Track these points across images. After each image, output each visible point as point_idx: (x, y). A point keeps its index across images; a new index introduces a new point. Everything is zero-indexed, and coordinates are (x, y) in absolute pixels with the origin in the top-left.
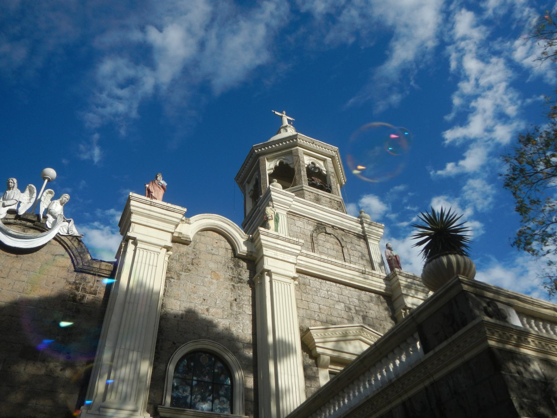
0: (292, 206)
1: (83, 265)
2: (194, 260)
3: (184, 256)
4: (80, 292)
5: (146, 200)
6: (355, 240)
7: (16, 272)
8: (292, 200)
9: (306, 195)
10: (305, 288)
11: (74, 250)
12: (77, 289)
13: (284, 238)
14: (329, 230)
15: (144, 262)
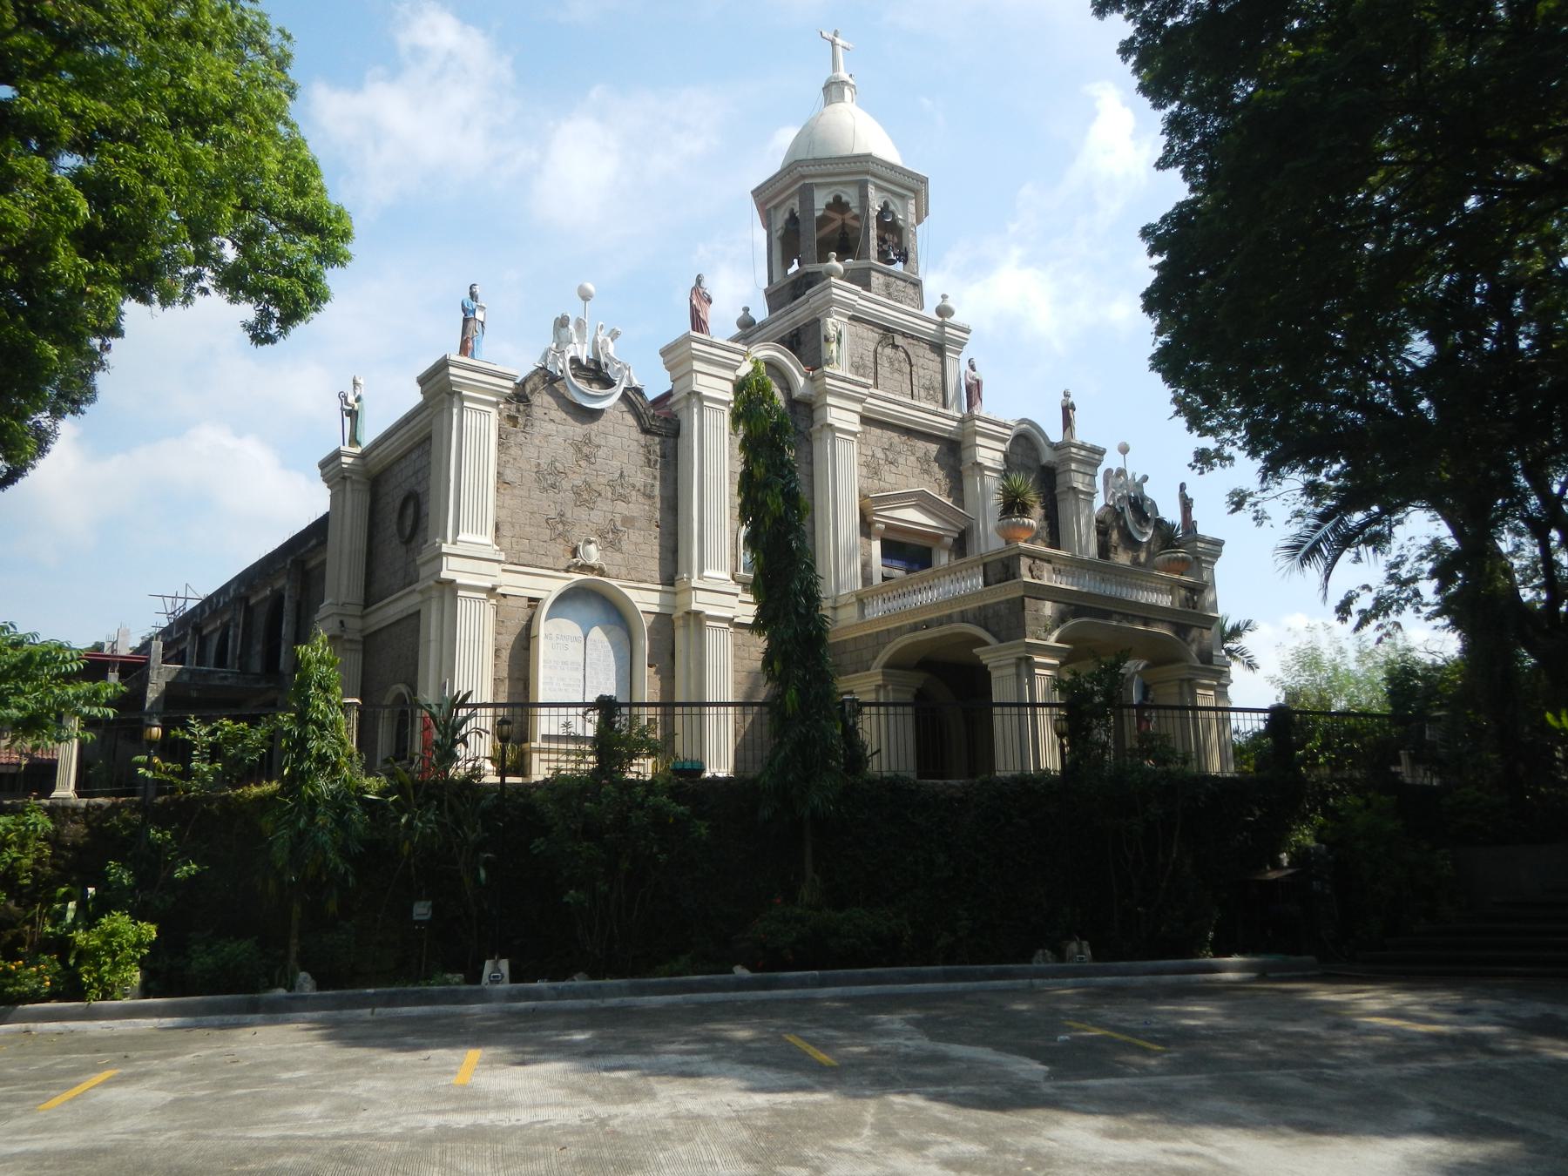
8: (856, 298)
11: (639, 405)
12: (649, 452)
14: (899, 340)
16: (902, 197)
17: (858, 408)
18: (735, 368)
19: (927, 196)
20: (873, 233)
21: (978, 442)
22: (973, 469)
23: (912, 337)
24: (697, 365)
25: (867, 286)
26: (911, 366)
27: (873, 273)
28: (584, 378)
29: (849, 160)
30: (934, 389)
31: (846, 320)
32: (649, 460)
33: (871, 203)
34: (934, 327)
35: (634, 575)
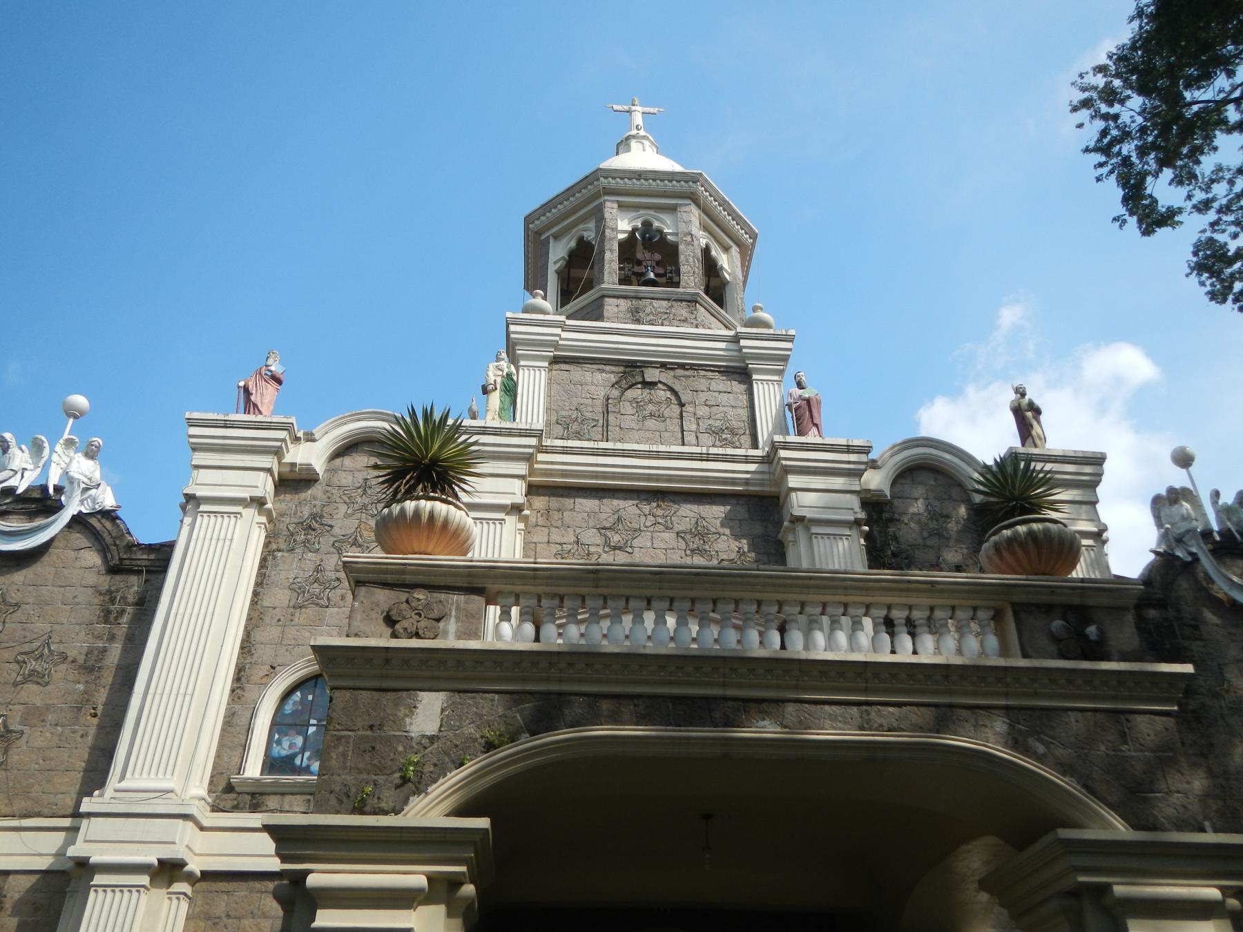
0: (561, 342)
1: (121, 559)
2: (324, 509)
3: (306, 505)
4: (116, 606)
5: (217, 420)
6: (720, 383)
7: (16, 591)
8: (558, 331)
9: (609, 308)
10: (561, 517)
11: (106, 535)
12: (112, 601)
13: (498, 428)
14: (652, 375)
15: (208, 536)
16: (673, 209)
17: (521, 468)
18: (278, 453)
19: (724, 204)
20: (611, 258)
21: (791, 485)
22: (793, 530)
23: (682, 366)
24: (200, 458)
25: (600, 317)
26: (682, 405)
27: (608, 300)
28: (23, 514)
29: (578, 188)
30: (733, 432)
31: (546, 364)
32: (109, 612)
33: (610, 224)
34: (722, 345)
35: (19, 805)
